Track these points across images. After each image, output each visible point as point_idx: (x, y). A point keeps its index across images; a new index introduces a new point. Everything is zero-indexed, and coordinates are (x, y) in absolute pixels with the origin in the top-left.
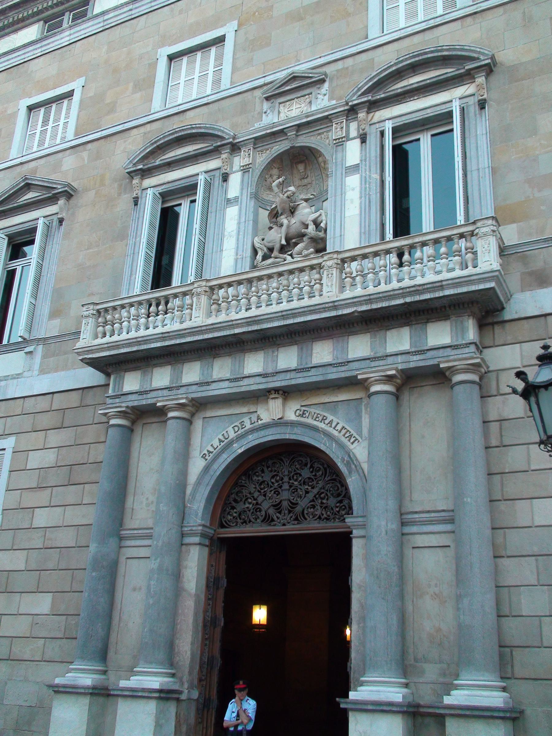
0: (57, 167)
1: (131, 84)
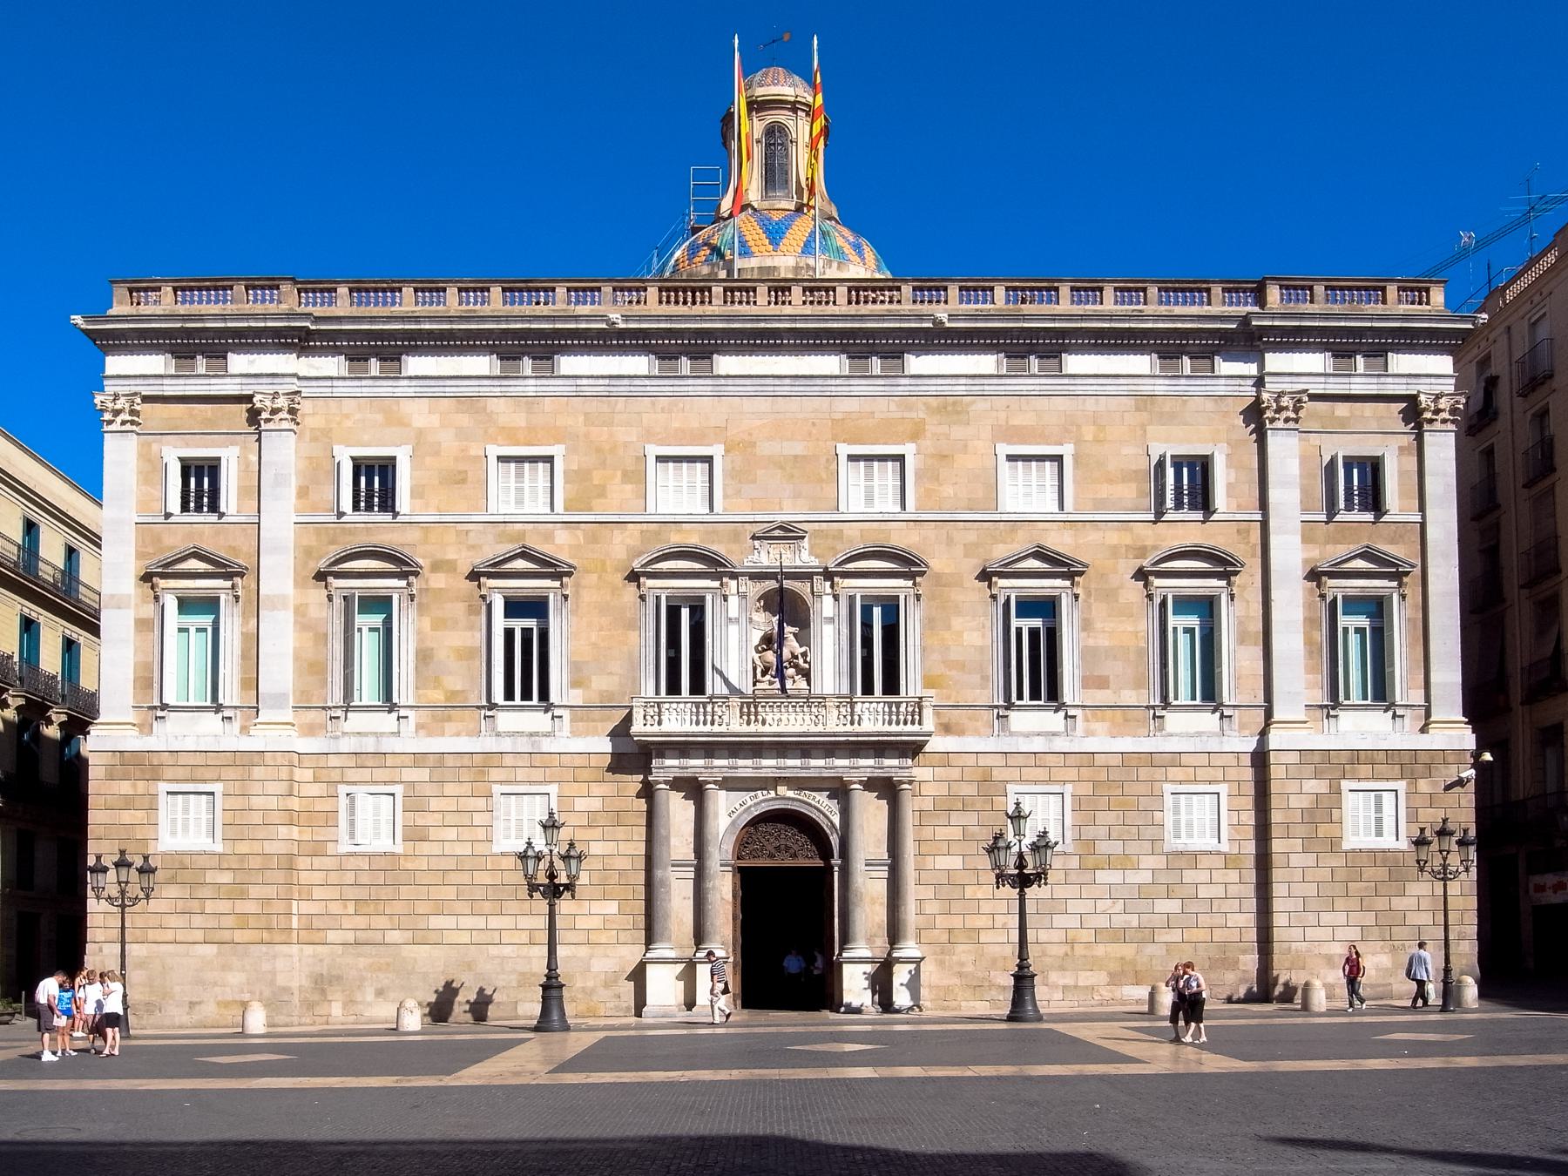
0: (549, 537)
1: (619, 473)
